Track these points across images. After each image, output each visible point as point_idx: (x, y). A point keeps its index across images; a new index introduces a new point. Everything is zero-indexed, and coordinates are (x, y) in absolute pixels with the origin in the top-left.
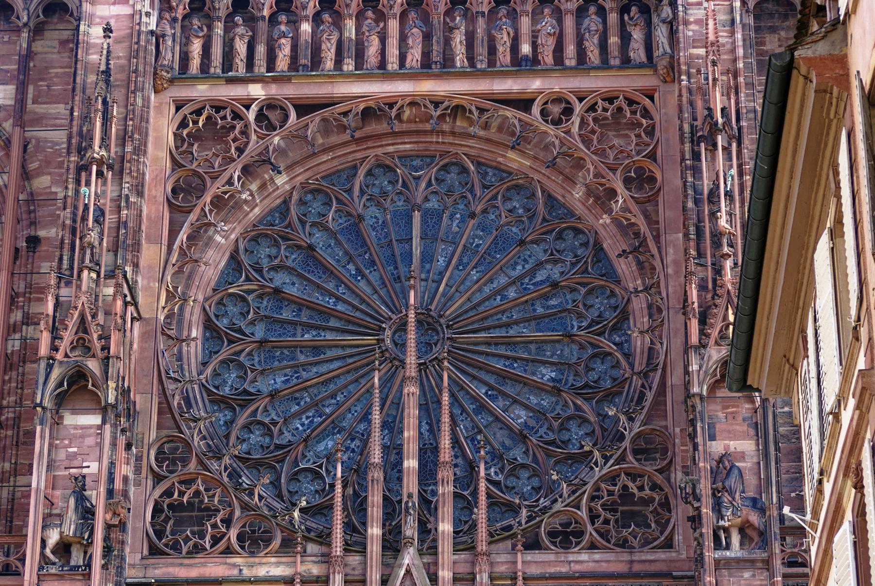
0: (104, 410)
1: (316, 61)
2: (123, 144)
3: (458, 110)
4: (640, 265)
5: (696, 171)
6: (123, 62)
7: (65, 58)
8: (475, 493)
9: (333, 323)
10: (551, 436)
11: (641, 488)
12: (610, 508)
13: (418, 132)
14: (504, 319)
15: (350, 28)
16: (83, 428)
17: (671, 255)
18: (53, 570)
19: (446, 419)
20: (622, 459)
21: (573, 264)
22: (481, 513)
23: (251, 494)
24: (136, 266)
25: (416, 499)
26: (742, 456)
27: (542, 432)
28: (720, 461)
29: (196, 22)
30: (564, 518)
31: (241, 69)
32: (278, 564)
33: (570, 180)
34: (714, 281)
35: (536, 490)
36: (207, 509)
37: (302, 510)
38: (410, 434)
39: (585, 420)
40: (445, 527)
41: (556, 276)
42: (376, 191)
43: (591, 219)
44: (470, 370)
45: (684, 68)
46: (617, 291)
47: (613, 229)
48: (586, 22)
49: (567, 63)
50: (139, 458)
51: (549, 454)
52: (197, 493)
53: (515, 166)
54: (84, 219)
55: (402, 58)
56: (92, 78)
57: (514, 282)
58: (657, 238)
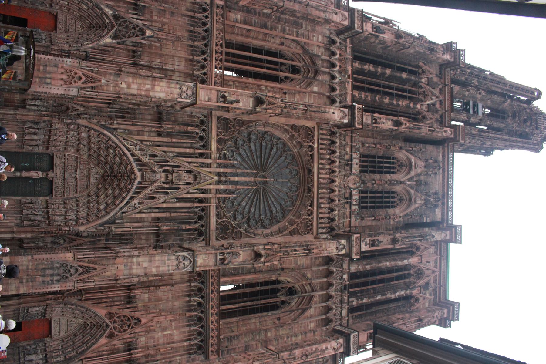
3: (310, 190)
5: (300, 246)
15: (328, 166)
20: (236, 228)
22: (225, 195)
24: (281, 117)
26: (239, 258)
28: (239, 253)
30: (222, 215)
38: (243, 179)
40: (222, 187)
43: (285, 220)
47: (283, 225)
50: (239, 115)
52: (231, 128)
56: (323, 109)
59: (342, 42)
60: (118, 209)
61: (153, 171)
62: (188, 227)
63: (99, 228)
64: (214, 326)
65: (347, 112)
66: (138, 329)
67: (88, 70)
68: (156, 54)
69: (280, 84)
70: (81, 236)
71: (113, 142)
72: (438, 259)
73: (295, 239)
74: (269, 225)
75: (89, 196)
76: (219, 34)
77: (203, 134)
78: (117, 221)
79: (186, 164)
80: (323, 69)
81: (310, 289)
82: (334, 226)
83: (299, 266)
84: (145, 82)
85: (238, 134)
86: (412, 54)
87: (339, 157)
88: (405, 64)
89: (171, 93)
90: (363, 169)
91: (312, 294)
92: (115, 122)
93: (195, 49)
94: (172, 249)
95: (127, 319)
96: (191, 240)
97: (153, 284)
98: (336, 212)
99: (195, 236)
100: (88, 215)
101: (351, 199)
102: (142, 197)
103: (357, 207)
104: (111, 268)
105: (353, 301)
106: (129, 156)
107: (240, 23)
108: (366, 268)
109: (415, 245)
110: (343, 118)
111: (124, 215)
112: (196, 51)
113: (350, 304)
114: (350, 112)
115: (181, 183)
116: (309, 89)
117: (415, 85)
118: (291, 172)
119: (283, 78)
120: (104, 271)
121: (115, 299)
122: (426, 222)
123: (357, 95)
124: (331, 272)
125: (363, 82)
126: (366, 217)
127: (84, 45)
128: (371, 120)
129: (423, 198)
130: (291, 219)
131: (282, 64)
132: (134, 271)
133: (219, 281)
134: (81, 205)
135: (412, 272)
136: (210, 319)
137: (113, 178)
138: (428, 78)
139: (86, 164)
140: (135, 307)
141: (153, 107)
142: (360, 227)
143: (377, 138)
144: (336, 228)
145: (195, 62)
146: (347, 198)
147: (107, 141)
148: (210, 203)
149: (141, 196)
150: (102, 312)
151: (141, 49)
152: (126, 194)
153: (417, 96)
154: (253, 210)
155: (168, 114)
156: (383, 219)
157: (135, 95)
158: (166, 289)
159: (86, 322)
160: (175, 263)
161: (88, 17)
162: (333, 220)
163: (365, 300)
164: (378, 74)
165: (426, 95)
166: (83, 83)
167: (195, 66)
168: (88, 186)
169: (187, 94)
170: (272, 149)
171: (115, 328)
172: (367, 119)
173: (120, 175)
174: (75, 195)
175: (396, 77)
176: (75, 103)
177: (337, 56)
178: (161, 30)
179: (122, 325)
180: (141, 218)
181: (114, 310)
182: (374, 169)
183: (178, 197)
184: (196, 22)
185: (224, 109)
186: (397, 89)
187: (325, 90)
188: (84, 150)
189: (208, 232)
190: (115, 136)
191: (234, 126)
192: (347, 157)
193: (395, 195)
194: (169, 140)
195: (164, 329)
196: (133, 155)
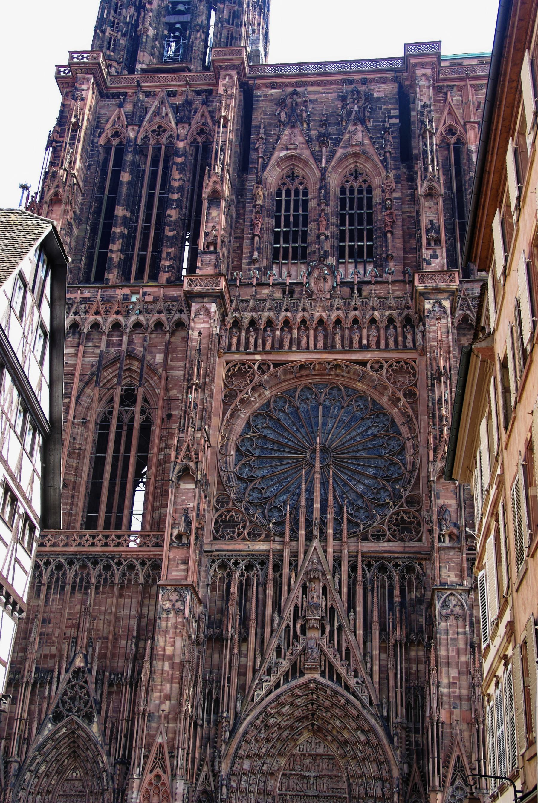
0: (196, 482)
1: (282, 346)
2: (205, 377)
3: (337, 366)
4: (410, 428)
5: (433, 391)
6: (206, 346)
7: (183, 344)
8: (342, 518)
9: (287, 449)
10: (373, 496)
11: (409, 518)
12: (395, 525)
13: (322, 375)
15: (295, 333)
16: (188, 489)
17: (422, 425)
18: (175, 545)
19: (331, 488)
20: (401, 506)
21: (383, 428)
22: (345, 526)
23: (253, 517)
24: (209, 426)
25: (318, 520)
26: (450, 506)
27: (369, 494)
28: (441, 507)
29: (235, 330)
30: (378, 529)
31: (252, 349)
32: (263, 544)
33: (382, 394)
34: (440, 435)
35: (367, 517)
36: (236, 522)
37: (273, 523)
38: (317, 494)
39: (387, 490)
40: (330, 531)
41: (376, 432)
42: (305, 397)
43: (390, 410)
44: (341, 469)
45: (428, 350)
46: (400, 438)
47: (399, 414)
48: (389, 331)
49: (381, 347)
50: (209, 502)
51: (372, 503)
52: (232, 516)
53: (360, 388)
54: (190, 407)
56: (193, 352)
57: (359, 435)
58: (417, 418)
59: (73, 310)
60: (365, 712)
62: (397, 592)
63: (396, 744)
65: (198, 306)
67: (145, 763)
68: (114, 647)
69: (153, 423)
70: (409, 774)
71: (257, 718)
72: (472, 82)
73: (422, 393)
78: (385, 713)
79: (292, 595)
80: (124, 347)
87: (277, 309)
88: (104, 173)
89: (176, 628)
90: (299, 257)
92: (225, 715)
100: (375, 760)
102: (345, 670)
104: (458, 732)
109: (444, 138)
110: (208, 312)
111: (375, 702)
112: (106, 579)
114: (196, 300)
115: (324, 604)
116: (160, 370)
117: (141, 151)
119: (144, 417)
120: (461, 744)
122: (400, 117)
123: (166, 275)
126: (387, 251)
127: (104, 767)
129: (351, 128)
131: (120, 420)
132: (464, 692)
137: (315, 716)
139: (295, 761)
141: (199, 652)
143: (243, 230)
144: (405, 314)
145: (123, 581)
146: (352, 291)
147: (256, 728)
148: (357, 552)
151: (107, 674)
152: (340, 698)
153: (163, 147)
155: (210, 625)
156: (391, 214)
160: (452, 621)
164: (126, 232)
165: (160, 127)
166: (165, 772)
167: (130, 581)
168: (331, 758)
169: (177, 601)
173: (310, 706)
174: (344, 779)
175: (128, 195)
176: (197, 780)
177: (99, 318)
178: (75, 641)
180: (381, 672)
183: (346, 608)
186: (152, 187)
188: (271, 764)
189: (407, 555)
190: (248, 715)
191: (229, 511)
192: (278, 295)
193: (348, 186)
194: (252, 624)
196: (277, 686)
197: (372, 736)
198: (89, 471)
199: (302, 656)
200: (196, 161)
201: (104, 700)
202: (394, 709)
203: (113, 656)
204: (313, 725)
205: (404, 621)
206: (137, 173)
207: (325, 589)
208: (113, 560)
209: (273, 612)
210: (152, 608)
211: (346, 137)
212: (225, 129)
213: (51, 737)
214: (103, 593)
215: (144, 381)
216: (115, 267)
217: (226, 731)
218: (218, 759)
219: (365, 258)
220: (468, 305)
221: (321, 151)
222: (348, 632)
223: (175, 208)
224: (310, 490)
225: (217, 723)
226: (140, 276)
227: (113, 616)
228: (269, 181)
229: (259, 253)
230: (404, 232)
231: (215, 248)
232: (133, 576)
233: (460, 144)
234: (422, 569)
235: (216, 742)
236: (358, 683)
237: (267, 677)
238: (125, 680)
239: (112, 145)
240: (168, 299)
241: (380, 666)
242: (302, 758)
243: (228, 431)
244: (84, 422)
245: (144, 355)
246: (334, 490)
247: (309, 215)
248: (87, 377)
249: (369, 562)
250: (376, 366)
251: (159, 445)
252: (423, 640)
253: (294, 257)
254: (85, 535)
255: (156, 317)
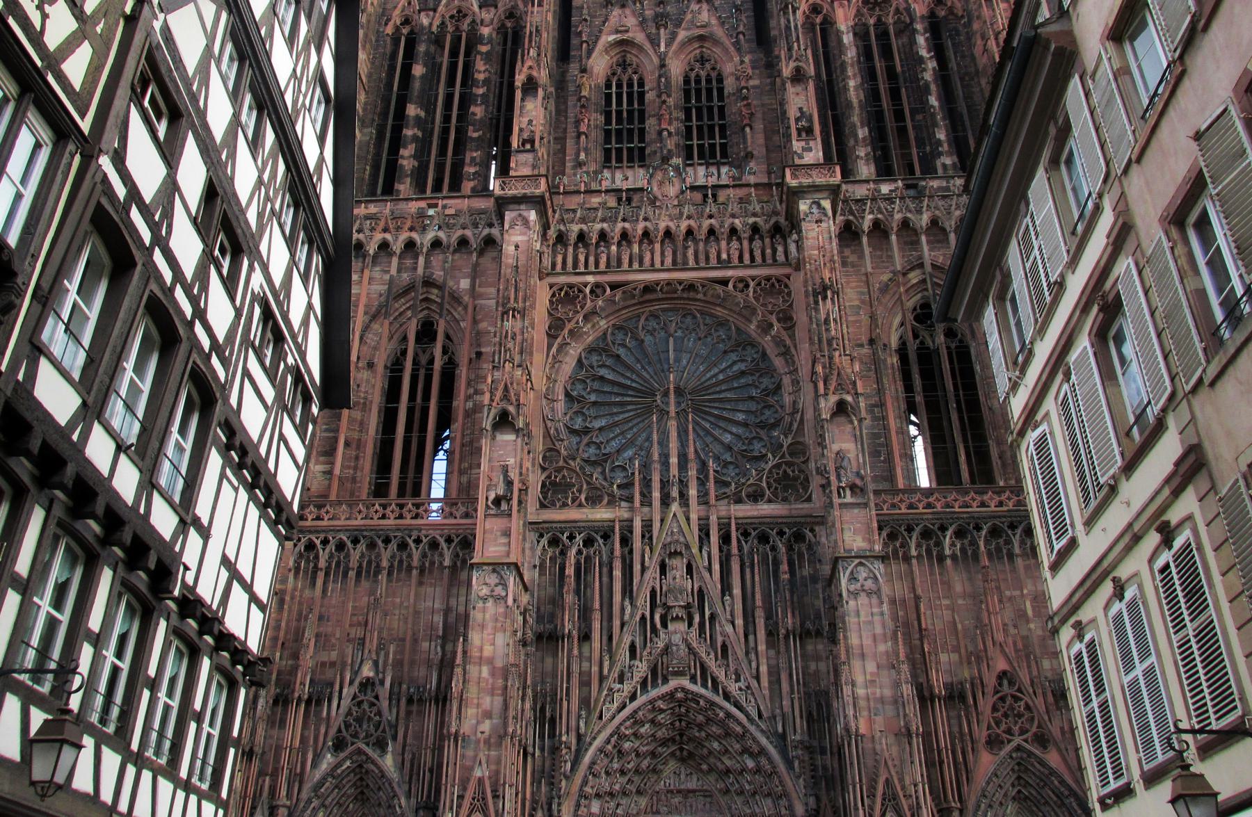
2: (525, 301)
3: (691, 287)
5: (817, 310)
11: (793, 471)
14: (718, 389)
15: (636, 248)
18: (492, 512)
20: (783, 456)
21: (752, 362)
22: (711, 485)
24: (531, 363)
26: (848, 451)
28: (838, 453)
30: (754, 488)
31: (582, 269)
34: (830, 363)
38: (674, 446)
39: (761, 439)
40: (693, 492)
41: (743, 368)
43: (760, 340)
47: (771, 344)
51: (743, 456)
52: (564, 476)
54: (506, 337)
55: (662, 263)
58: (795, 347)
60: (752, 729)
61: (666, 650)
62: (784, 567)
63: (797, 770)
64: (1009, 499)
65: (514, 214)
66: (1024, 676)
70: (817, 811)
71: (608, 741)
73: (801, 317)
74: (773, 376)
75: (727, 792)
76: (360, 512)
77: (579, 539)
78: (780, 729)
79: (648, 575)
80: (420, 270)
81: (918, 272)
82: (768, 226)
83: (863, 302)
84: (476, 680)
85: (574, 459)
86: (369, 55)
87: (612, 220)
88: (392, 68)
90: (636, 159)
91: (928, 268)
92: (564, 738)
93: (396, 564)
94: (836, 604)
95: (1000, 704)
96: (815, 560)
97: (918, 642)
98: (737, 221)
99: (804, 548)
100: (769, 795)
101: (705, 187)
102: (723, 673)
103: (724, 170)
105: (944, 165)
106: (636, 704)
107: (333, 463)
108: (864, 139)
109: (808, 17)
110: (526, 222)
111: (765, 715)
113: (951, 173)
114: (511, 207)
116: (466, 298)
117: (438, 41)
118: (651, 333)
119: (446, 357)
121: (956, 729)
123: (472, 184)
124: (876, 224)
125: (440, 167)
126: (746, 148)
128: (525, 155)
130: (758, 327)
133: (903, 491)
134: (748, 811)
135: (872, 21)
136: (993, 508)
137: (685, 738)
138: (419, 12)
139: (659, 800)
140: (972, 684)
141: (527, 655)
142: (768, 158)
143: (565, 129)
145: (424, 563)
146: (706, 196)
147: (606, 755)
148: (730, 518)
149: (720, 674)
150: (986, 763)
151: (404, 686)
152: (718, 711)
153: (464, 35)
154: (740, 417)
155: (540, 619)
157: (505, 701)
158: (928, 612)
159: (1014, 798)
161: (341, 806)
162: (755, 229)
163: (941, 135)
165: (459, 11)
167: (432, 563)
170: (602, 378)
171: (1023, 731)
172: (521, 164)
173: (677, 724)
175: (422, 90)
177: (388, 236)
179: (1015, 716)
180: (770, 673)
181: (981, 734)
182: (636, 131)
184: (338, 564)
185: (523, 496)
186: (451, 82)
187: (465, 262)
190: (595, 738)
192: (612, 203)
193: (693, 75)
195: (1022, 614)
196: (633, 697)
197: (763, 761)
198: (378, 426)
199: (665, 656)
200: (504, 50)
201: (401, 722)
202: (791, 724)
203: (412, 663)
204: (681, 749)
205: (796, 605)
206: (434, 69)
207: (689, 568)
208: (410, 537)
209: (623, 599)
210: (462, 599)
211: (689, 16)
212: (540, 9)
213: (331, 773)
214: (398, 580)
215: (445, 312)
216: (407, 176)
217: (566, 762)
218: (556, 800)
219: (718, 158)
220: (851, 208)
221: (659, 34)
222: (724, 622)
223: (480, 105)
224: (663, 443)
225: (555, 750)
226: (437, 187)
227: (411, 610)
228: (595, 70)
229: (586, 155)
230: (765, 127)
231: (533, 146)
232: (436, 558)
233: (828, 24)
234: (815, 536)
235: (553, 777)
236: (740, 689)
237: (619, 686)
238: (429, 693)
239: (402, 34)
240: (472, 212)
241: (768, 665)
242: (669, 795)
243: (554, 370)
244: (371, 365)
245: (445, 280)
246: (695, 442)
247: (647, 109)
248: (374, 309)
249: (746, 531)
250: (741, 285)
251: (466, 392)
252: (823, 629)
253: (630, 160)
254: (374, 505)
255: (459, 233)
